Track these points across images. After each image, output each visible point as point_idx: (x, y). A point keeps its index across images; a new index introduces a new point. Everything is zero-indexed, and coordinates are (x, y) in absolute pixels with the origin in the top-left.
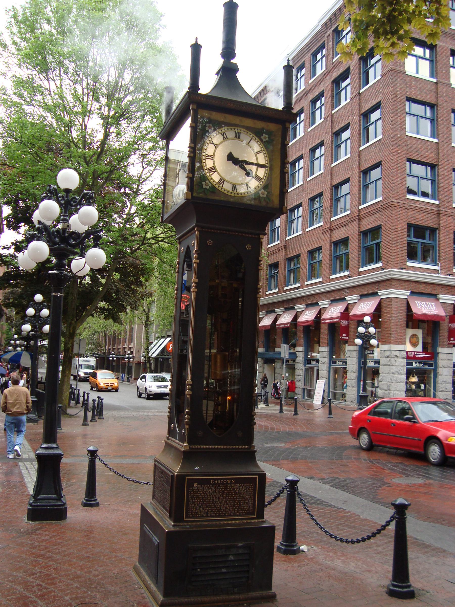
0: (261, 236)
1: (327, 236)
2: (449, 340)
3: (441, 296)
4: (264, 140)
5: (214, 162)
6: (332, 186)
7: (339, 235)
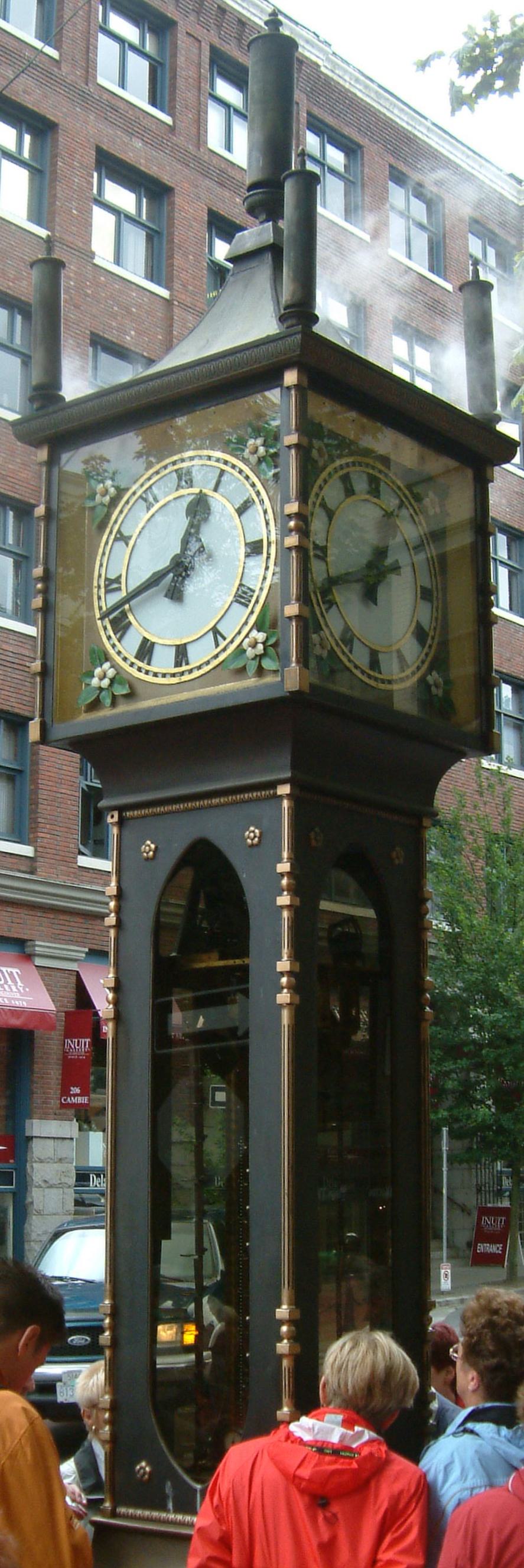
2: (65, 1092)
3: (41, 946)
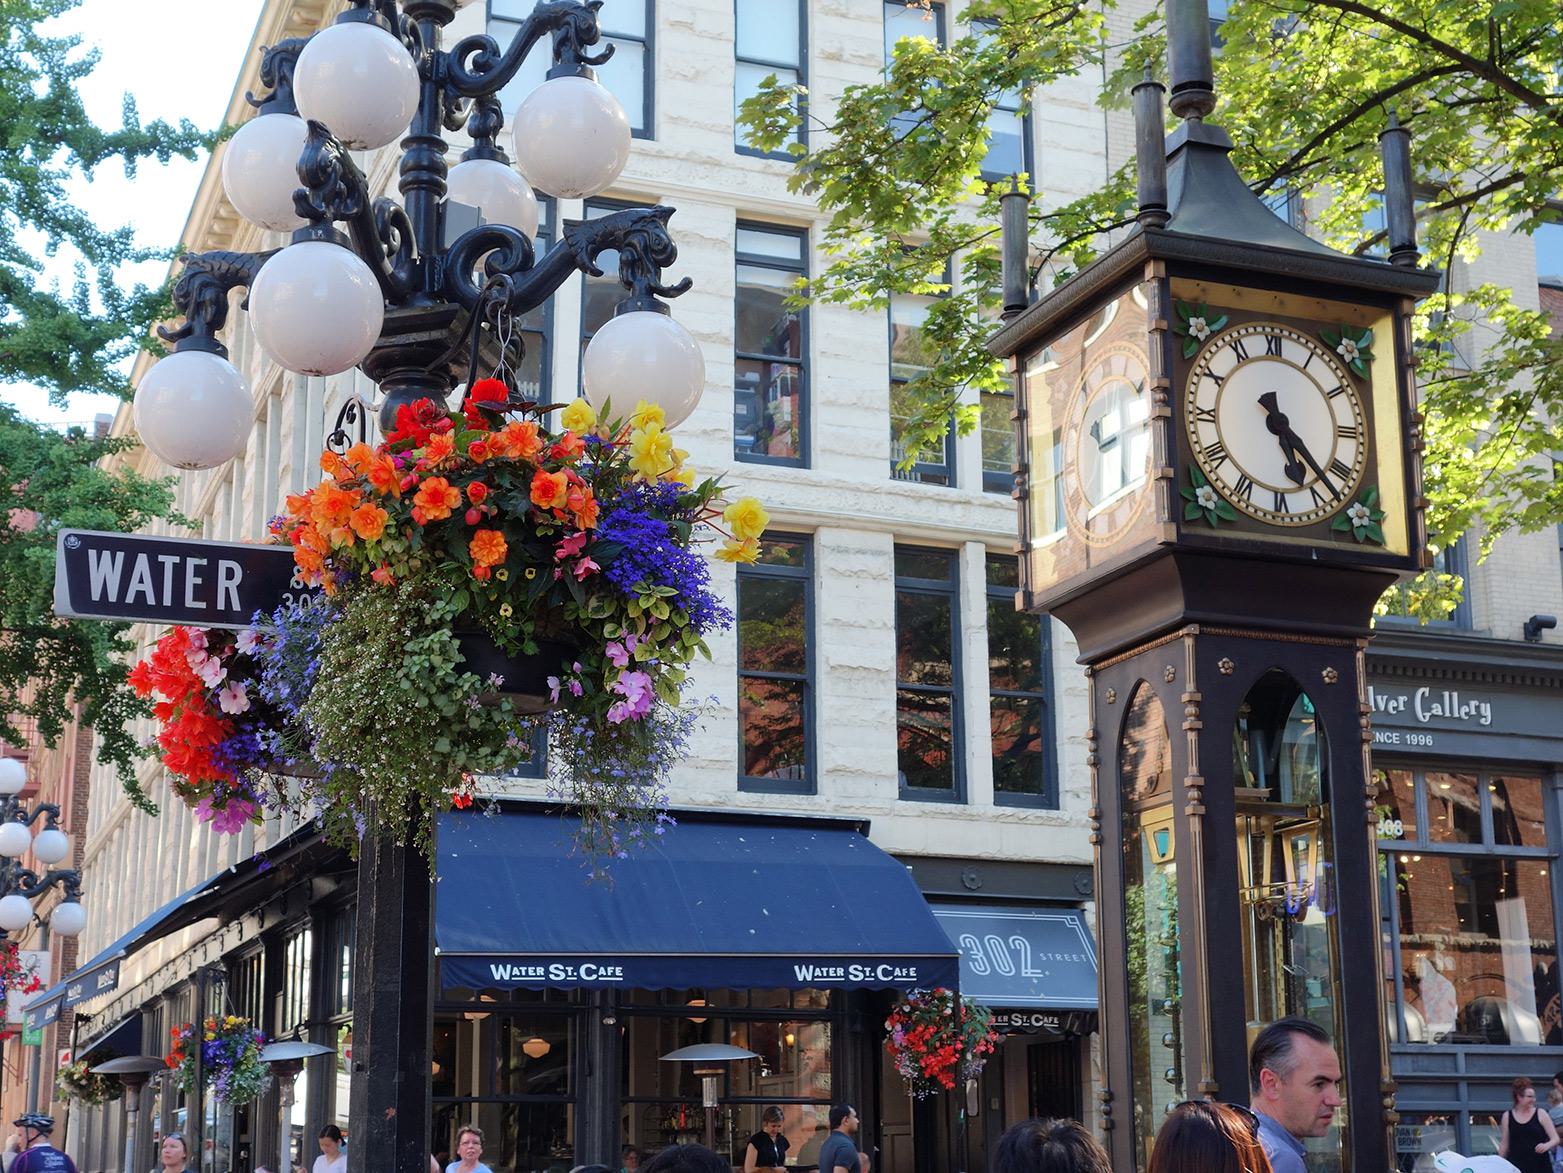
4: (1348, 358)
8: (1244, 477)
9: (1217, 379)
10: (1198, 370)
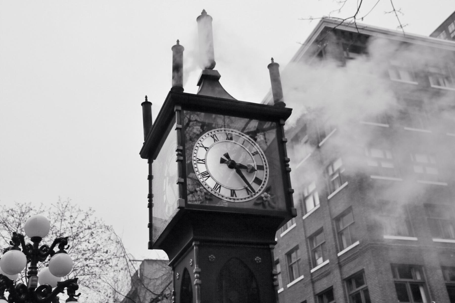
0: (271, 246)
1: (310, 288)
5: (206, 167)
6: (307, 238)
7: (322, 286)
8: (217, 184)
9: (205, 148)
10: (198, 145)
